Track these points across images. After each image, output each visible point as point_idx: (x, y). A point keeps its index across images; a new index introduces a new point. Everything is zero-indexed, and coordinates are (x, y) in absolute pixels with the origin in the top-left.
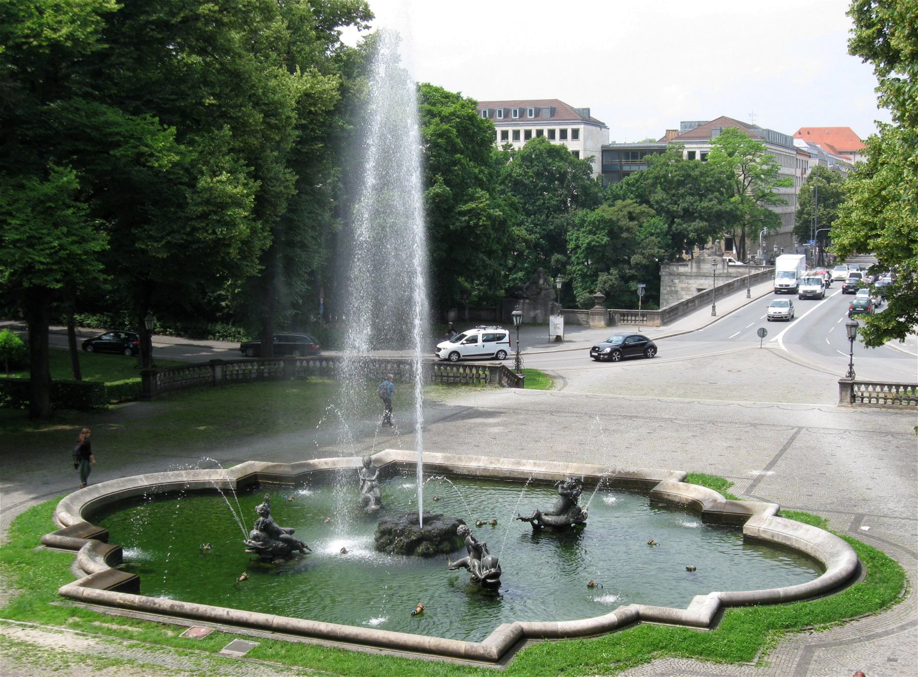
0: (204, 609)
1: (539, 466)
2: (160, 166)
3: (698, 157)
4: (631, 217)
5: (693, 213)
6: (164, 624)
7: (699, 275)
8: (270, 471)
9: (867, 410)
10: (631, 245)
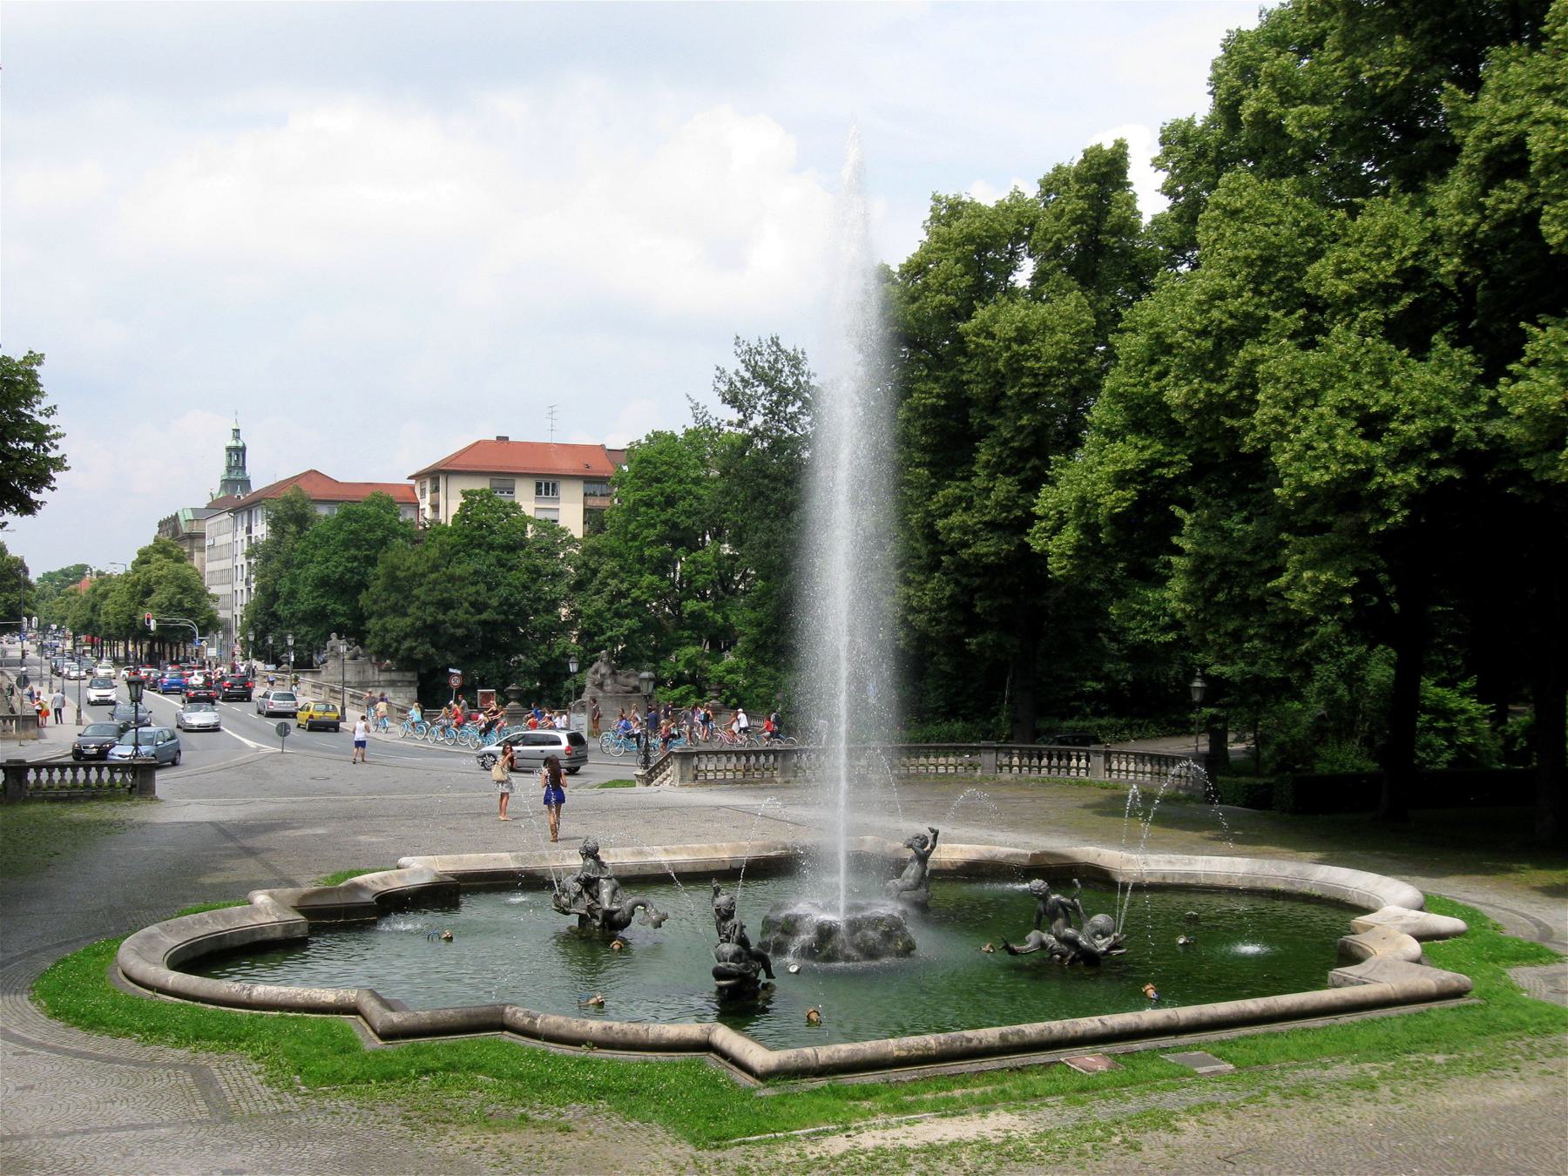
1: (675, 853)
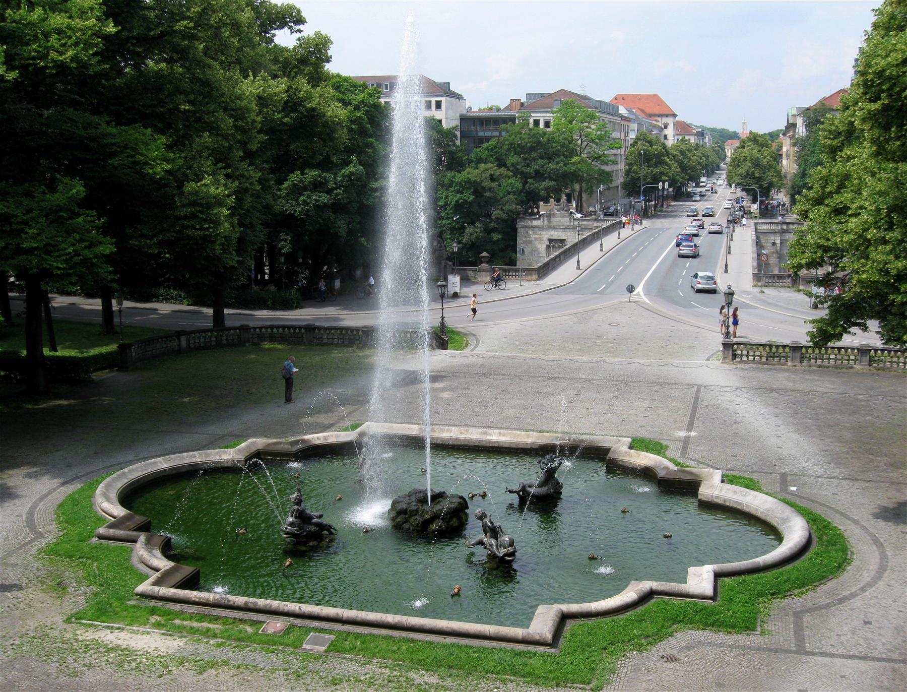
0: (277, 605)
1: (504, 435)
2: (155, 173)
3: (542, 125)
4: (493, 179)
5: (543, 174)
6: (240, 620)
7: (549, 228)
8: (272, 448)
9: (747, 366)
10: (494, 202)
